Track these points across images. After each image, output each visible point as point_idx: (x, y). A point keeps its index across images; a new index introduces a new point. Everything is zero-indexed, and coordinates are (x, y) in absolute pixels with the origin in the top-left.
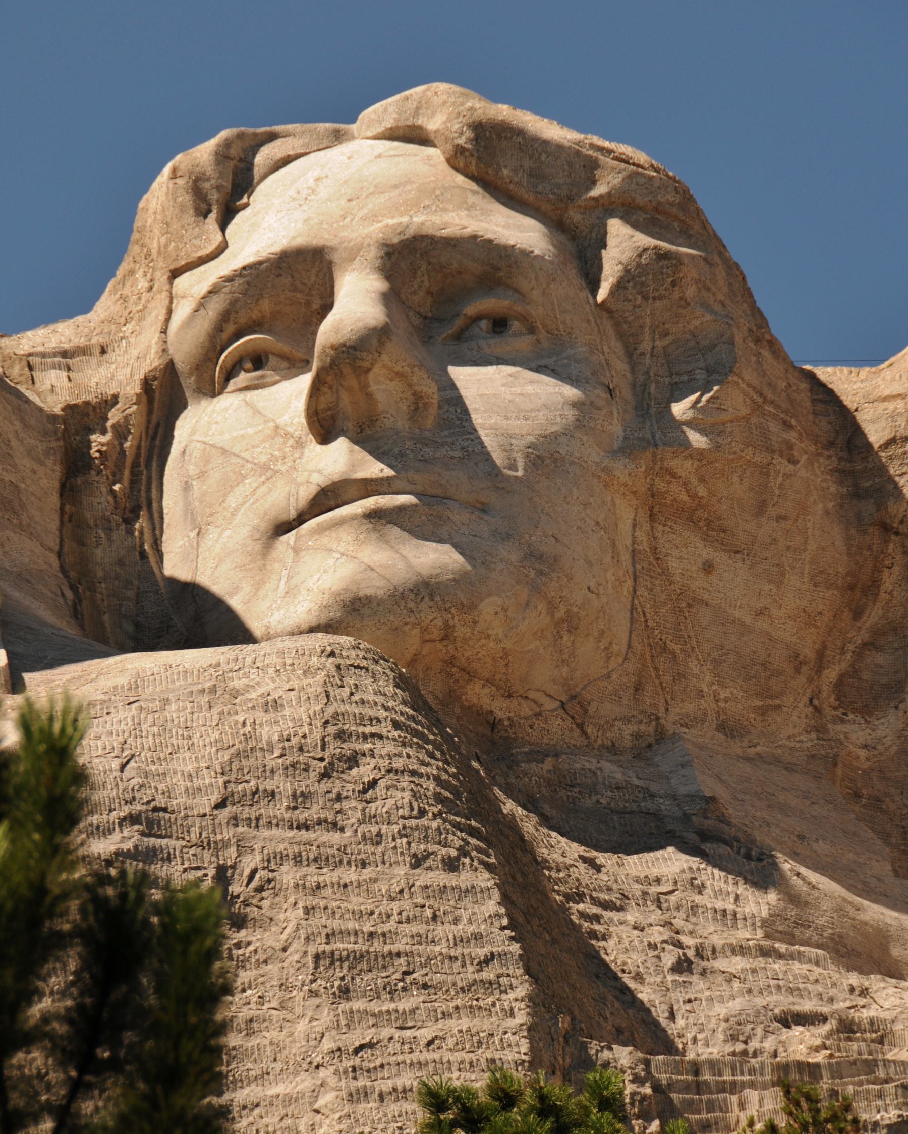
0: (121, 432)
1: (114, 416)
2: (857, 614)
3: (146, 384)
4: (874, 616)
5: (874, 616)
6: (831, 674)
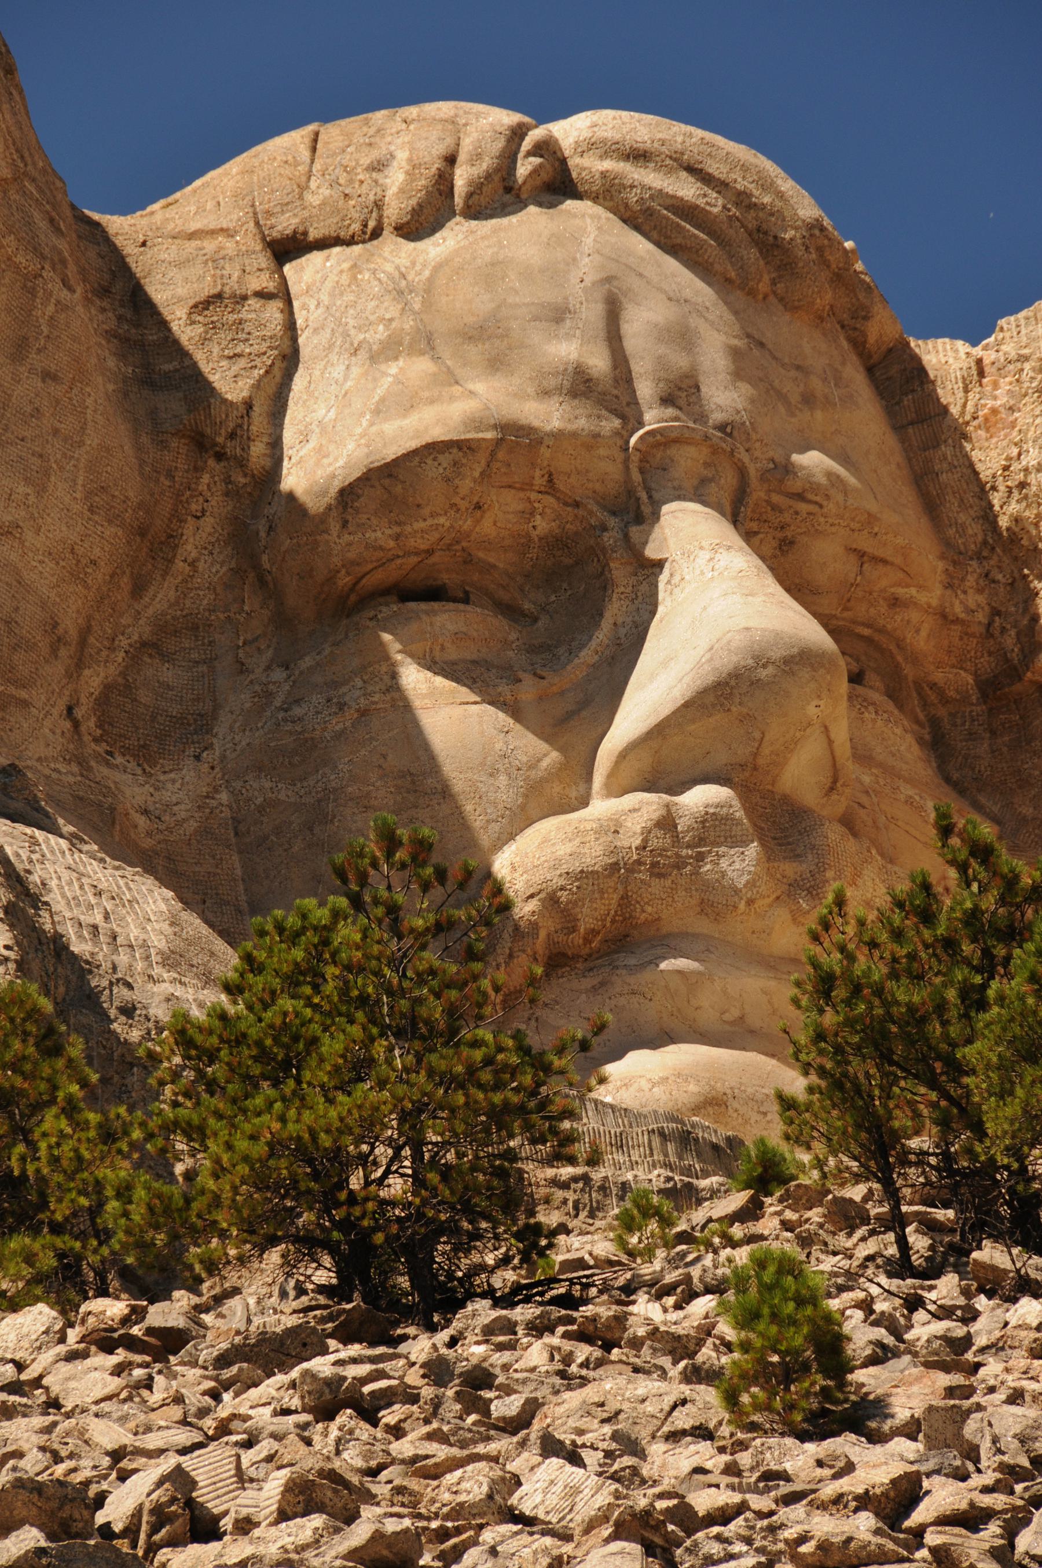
2: (138, 589)
4: (161, 598)
5: (161, 598)
6: (93, 680)
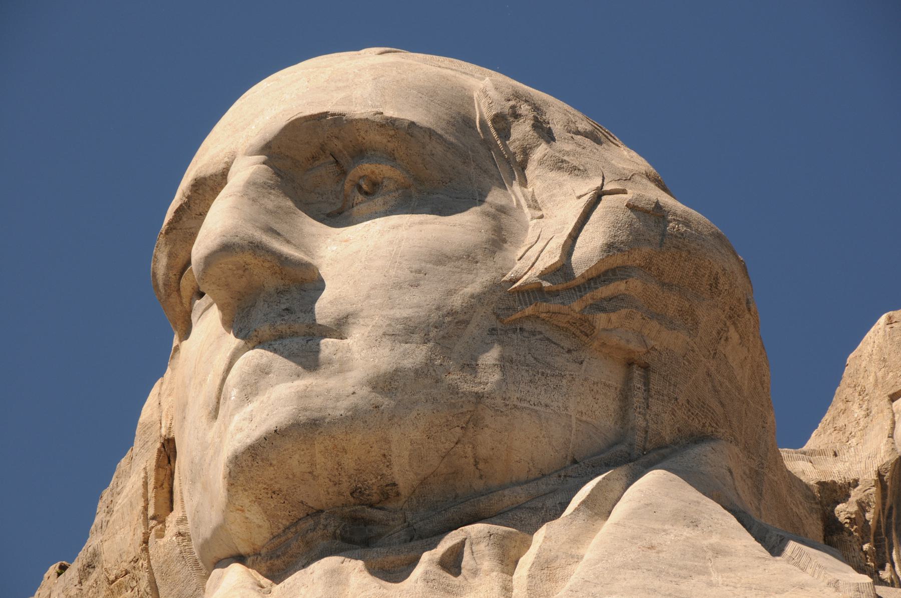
0: (863, 507)
1: (855, 495)
3: (879, 475)
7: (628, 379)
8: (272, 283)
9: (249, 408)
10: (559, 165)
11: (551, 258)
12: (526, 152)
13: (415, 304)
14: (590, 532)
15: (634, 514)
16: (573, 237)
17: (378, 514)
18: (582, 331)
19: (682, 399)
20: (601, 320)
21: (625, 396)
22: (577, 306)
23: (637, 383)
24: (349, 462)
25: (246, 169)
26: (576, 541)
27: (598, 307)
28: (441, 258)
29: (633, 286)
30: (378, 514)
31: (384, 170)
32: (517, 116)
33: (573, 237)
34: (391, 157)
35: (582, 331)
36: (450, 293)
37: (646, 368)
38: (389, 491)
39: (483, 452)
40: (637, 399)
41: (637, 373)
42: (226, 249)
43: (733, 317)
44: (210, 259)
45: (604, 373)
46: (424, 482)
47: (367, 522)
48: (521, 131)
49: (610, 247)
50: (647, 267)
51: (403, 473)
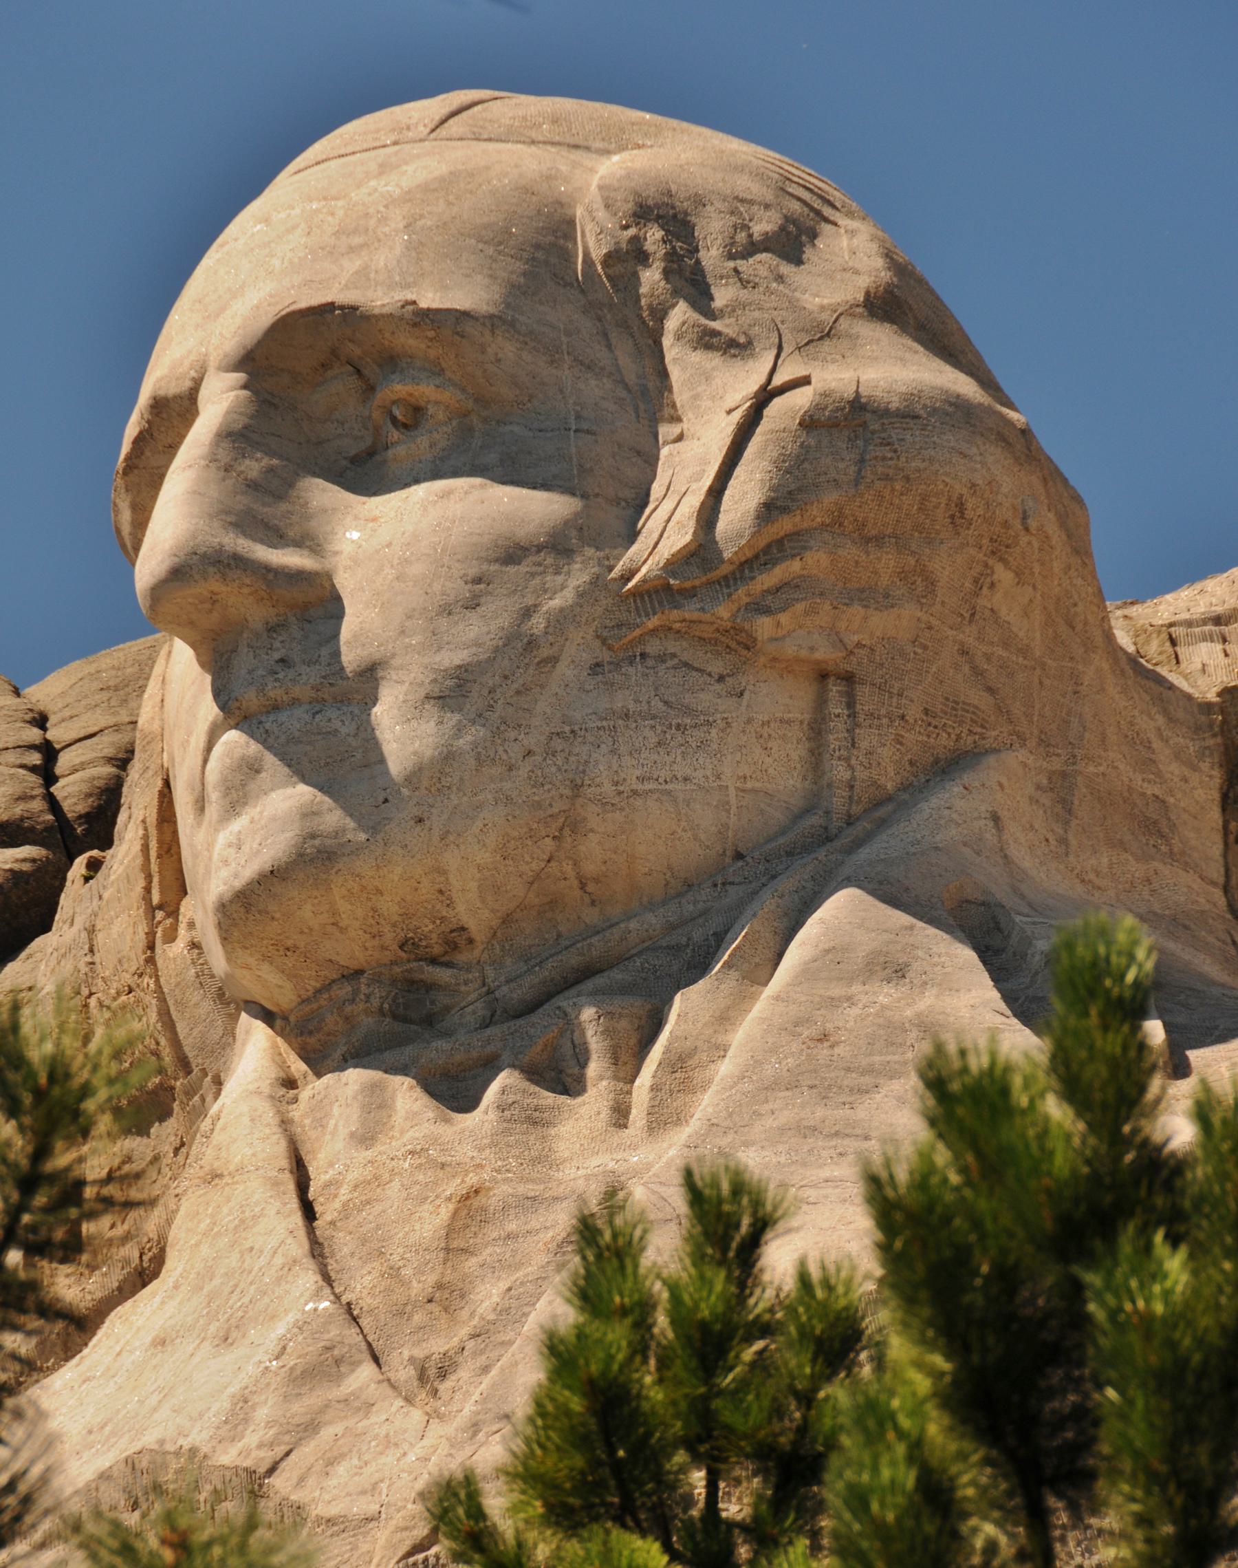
7: (821, 702)
8: (257, 614)
9: (239, 824)
10: (707, 341)
11: (679, 538)
12: (660, 314)
13: (471, 637)
14: (743, 1000)
15: (808, 973)
16: (716, 492)
17: (443, 975)
18: (738, 643)
19: (913, 713)
20: (764, 626)
21: (817, 730)
22: (724, 611)
23: (836, 708)
24: (389, 906)
25: (220, 401)
26: (726, 1019)
27: (759, 608)
28: (513, 553)
29: (815, 561)
30: (443, 975)
31: (426, 391)
32: (641, 257)
33: (716, 492)
34: (436, 370)
35: (738, 643)
36: (527, 613)
37: (849, 679)
38: (456, 939)
39: (590, 868)
40: (836, 737)
41: (835, 689)
42: (178, 574)
43: (999, 549)
44: (158, 591)
45: (779, 700)
46: (507, 920)
47: (430, 987)
48: (651, 278)
49: (769, 510)
50: (836, 523)
51: (473, 912)
